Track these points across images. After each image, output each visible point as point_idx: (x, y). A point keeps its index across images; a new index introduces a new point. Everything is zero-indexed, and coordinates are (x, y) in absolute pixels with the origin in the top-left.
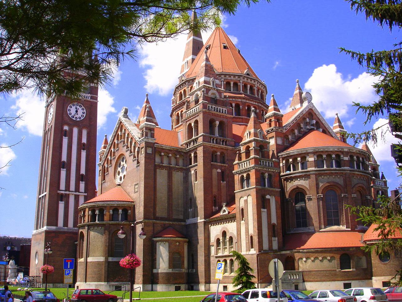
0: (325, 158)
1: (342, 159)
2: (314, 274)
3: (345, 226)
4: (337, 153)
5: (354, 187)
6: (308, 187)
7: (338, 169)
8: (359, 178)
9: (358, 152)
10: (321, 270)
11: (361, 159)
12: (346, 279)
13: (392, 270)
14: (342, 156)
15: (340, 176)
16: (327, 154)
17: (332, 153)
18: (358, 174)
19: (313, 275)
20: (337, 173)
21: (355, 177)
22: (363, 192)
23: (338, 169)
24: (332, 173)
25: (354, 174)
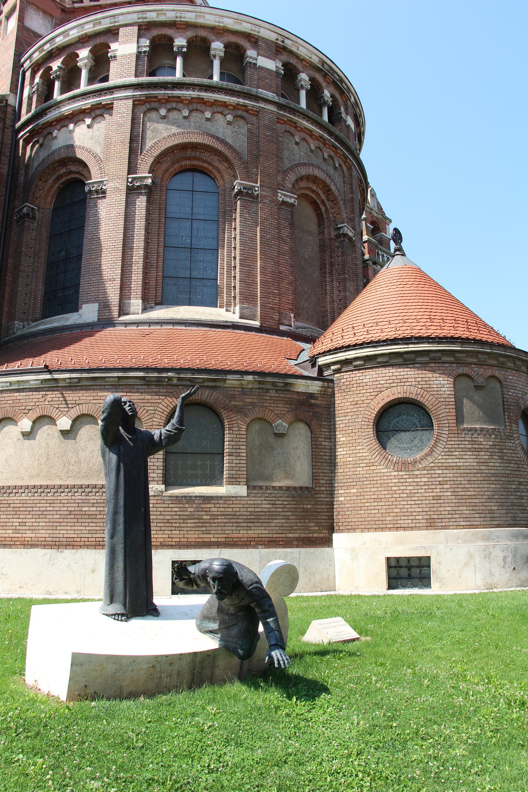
0: (183, 47)
1: (254, 62)
2: (24, 503)
3: (237, 308)
4: (233, 39)
5: (292, 168)
6: (98, 150)
7: (225, 84)
8: (313, 148)
9: (315, 60)
10: (58, 482)
11: (327, 93)
12: (193, 536)
13: (439, 498)
14: (251, 53)
15: (236, 117)
16: (190, 34)
17: (210, 36)
18: (311, 133)
19: (16, 512)
20: (225, 105)
21: (297, 139)
22: (327, 210)
23: (225, 84)
24: (201, 100)
25: (295, 125)
